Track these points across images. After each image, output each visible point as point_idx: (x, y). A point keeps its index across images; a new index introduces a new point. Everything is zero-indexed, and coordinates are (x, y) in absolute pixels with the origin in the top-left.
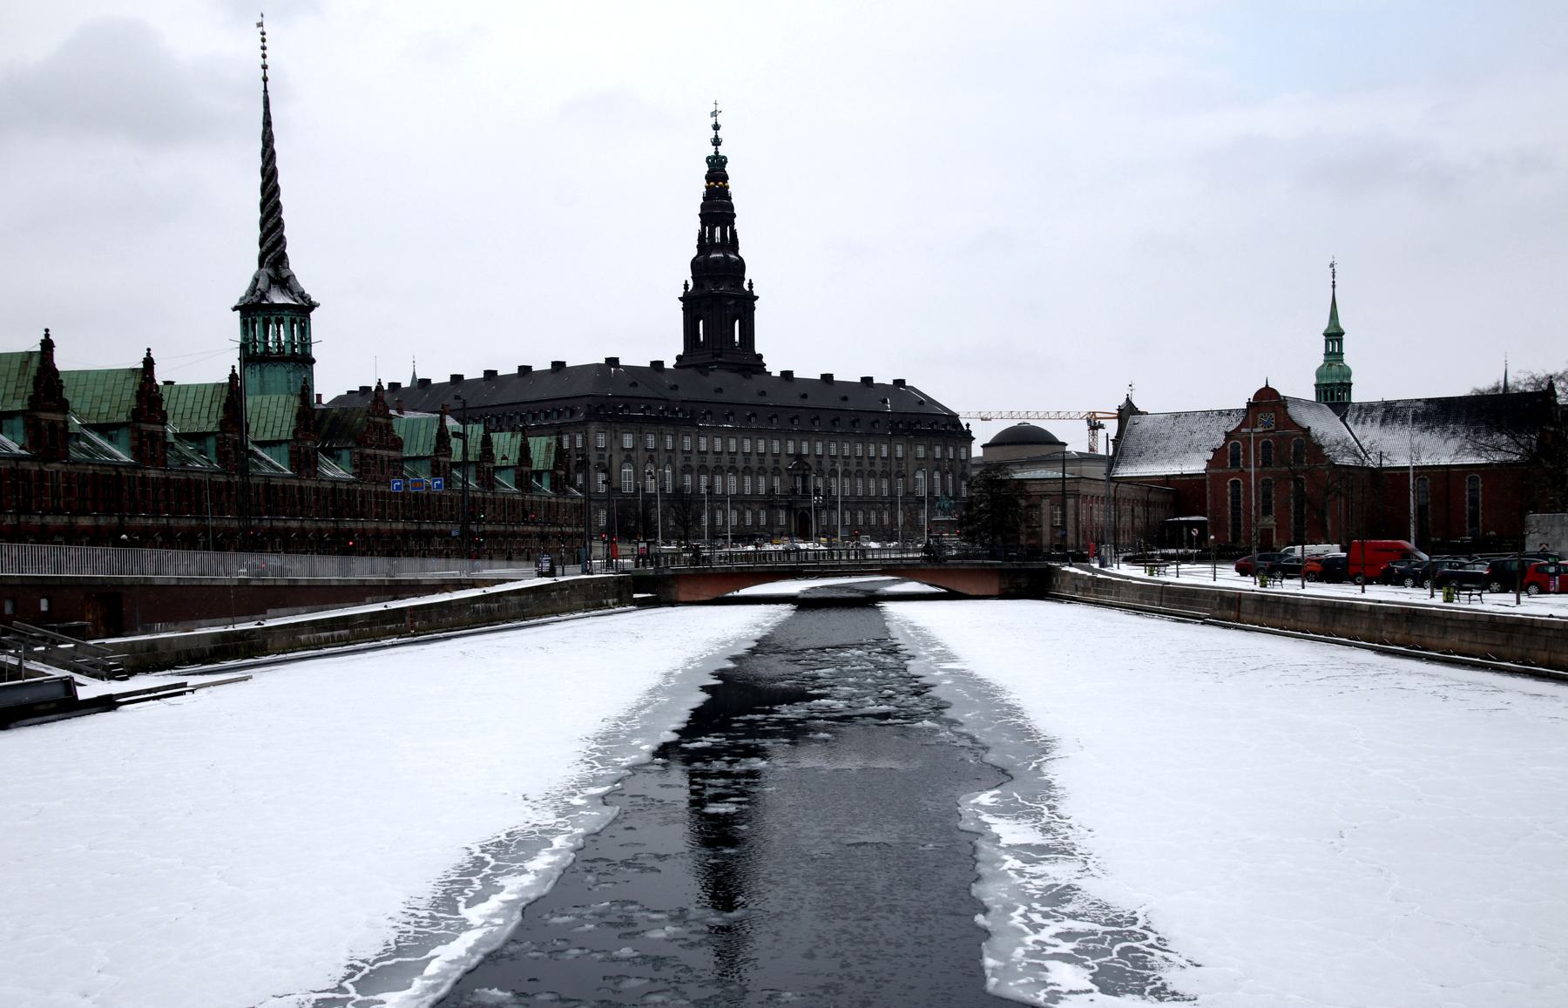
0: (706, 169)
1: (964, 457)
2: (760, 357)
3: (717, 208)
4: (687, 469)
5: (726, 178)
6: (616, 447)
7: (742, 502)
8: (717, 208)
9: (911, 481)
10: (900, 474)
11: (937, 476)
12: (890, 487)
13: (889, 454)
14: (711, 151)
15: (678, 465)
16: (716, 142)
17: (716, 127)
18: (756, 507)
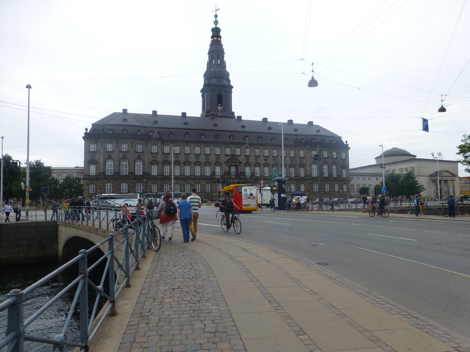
0: (211, 34)
1: (344, 157)
2: (234, 113)
3: (216, 50)
4: (154, 162)
5: (221, 37)
6: (102, 150)
7: (193, 179)
8: (216, 50)
9: (309, 169)
10: (302, 166)
11: (325, 167)
12: (296, 172)
13: (295, 155)
14: (214, 26)
15: (146, 159)
16: (216, 22)
17: (216, 16)
18: (203, 182)
